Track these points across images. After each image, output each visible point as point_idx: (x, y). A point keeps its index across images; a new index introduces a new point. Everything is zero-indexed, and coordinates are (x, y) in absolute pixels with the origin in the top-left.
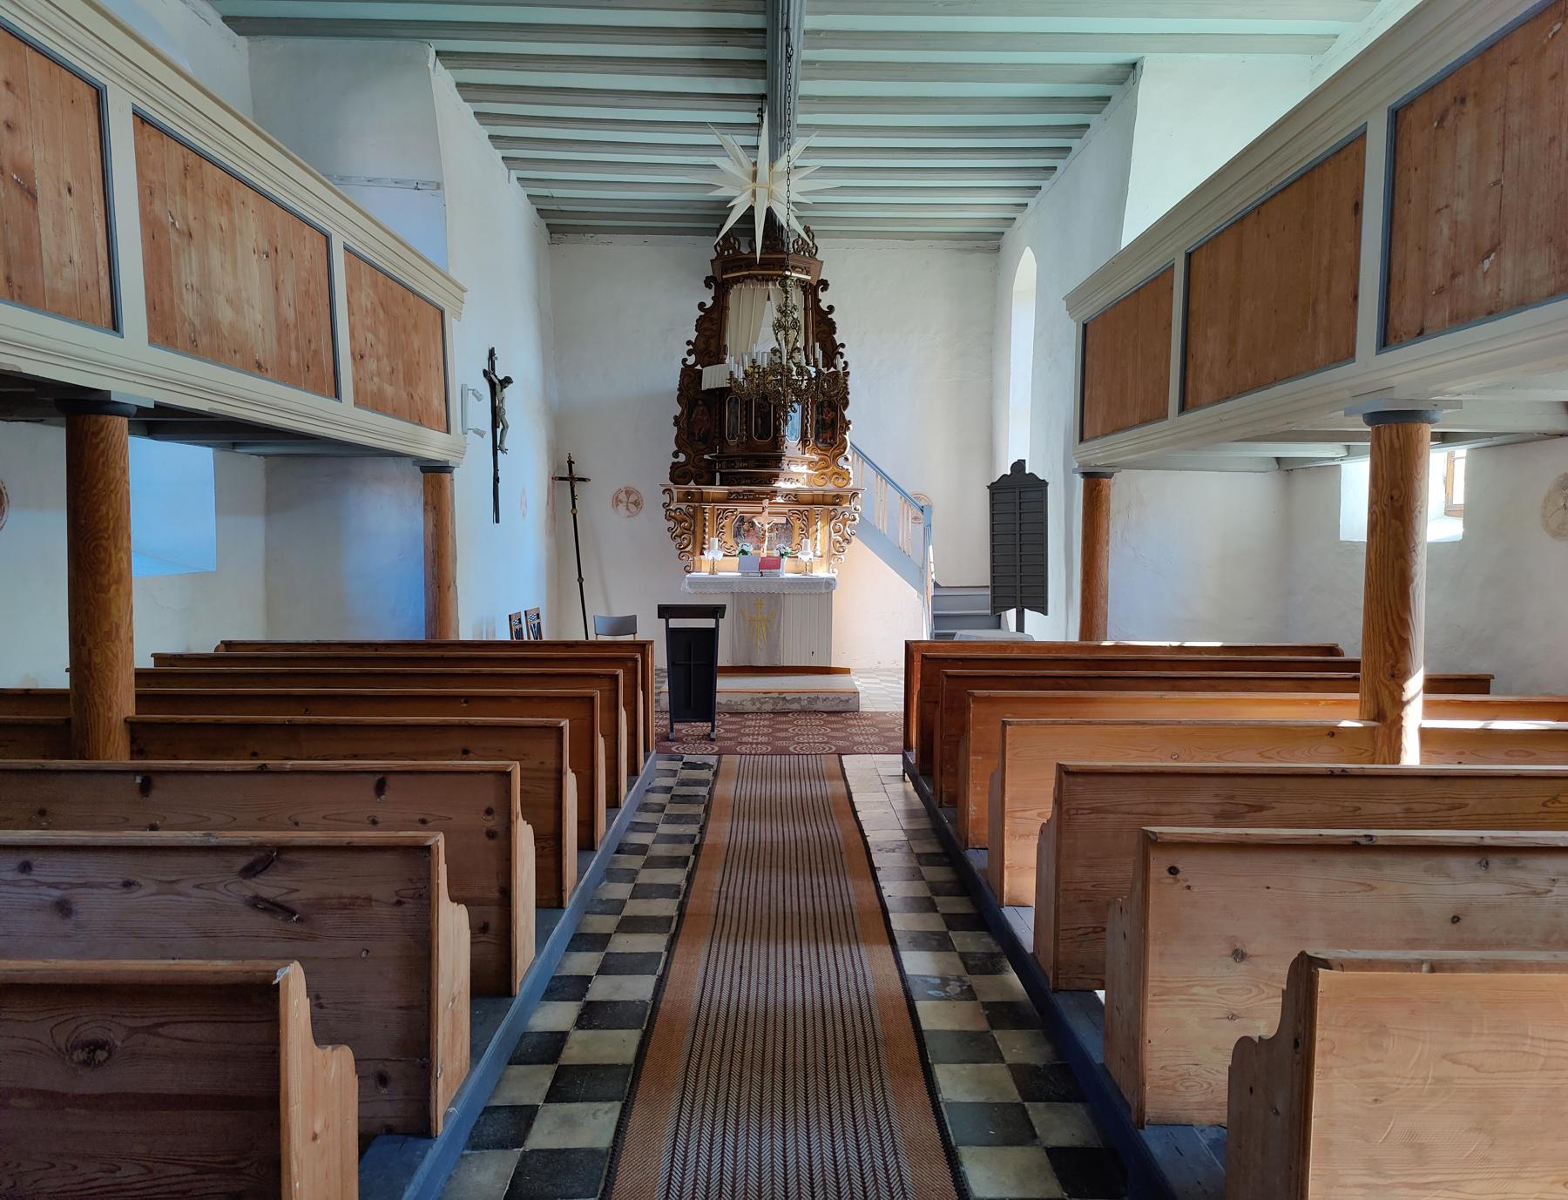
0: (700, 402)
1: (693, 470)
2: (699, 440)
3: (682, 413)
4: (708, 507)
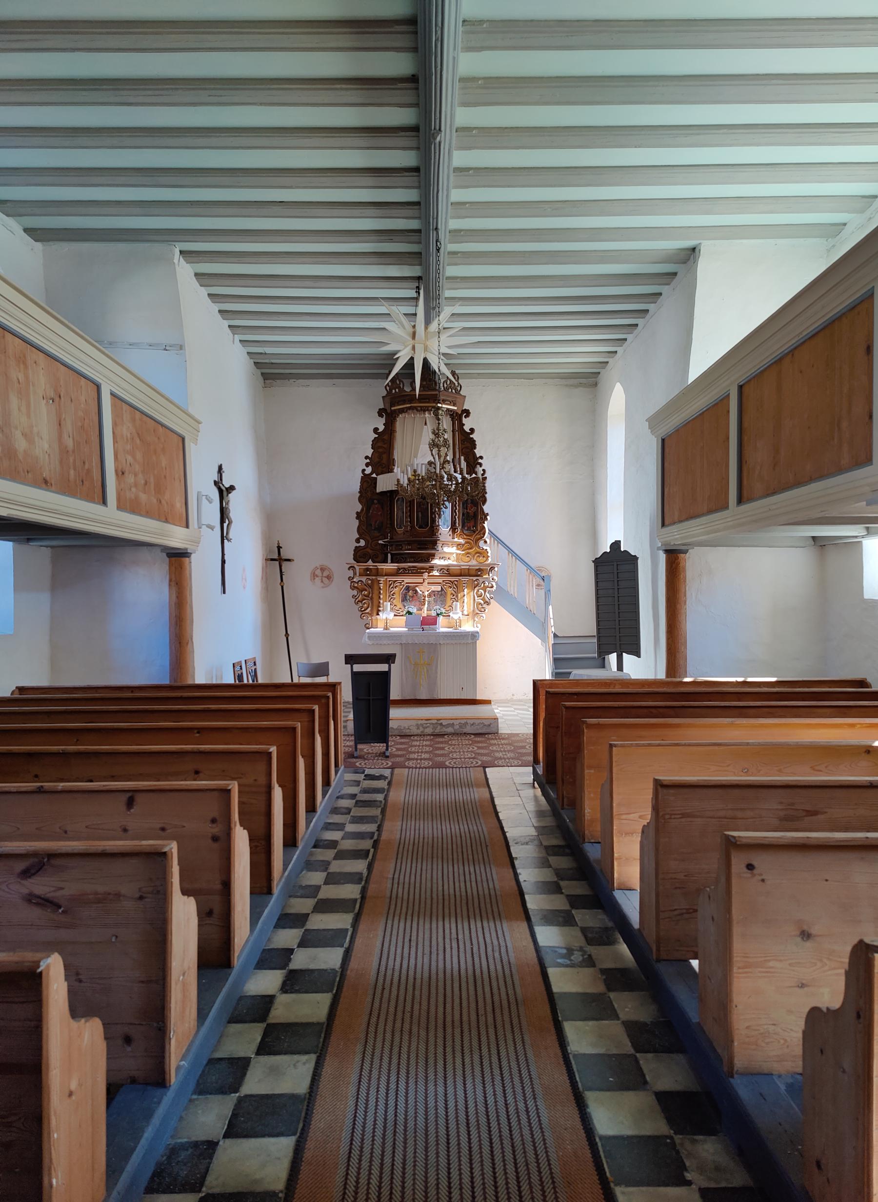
0: (375, 501)
3: (362, 510)
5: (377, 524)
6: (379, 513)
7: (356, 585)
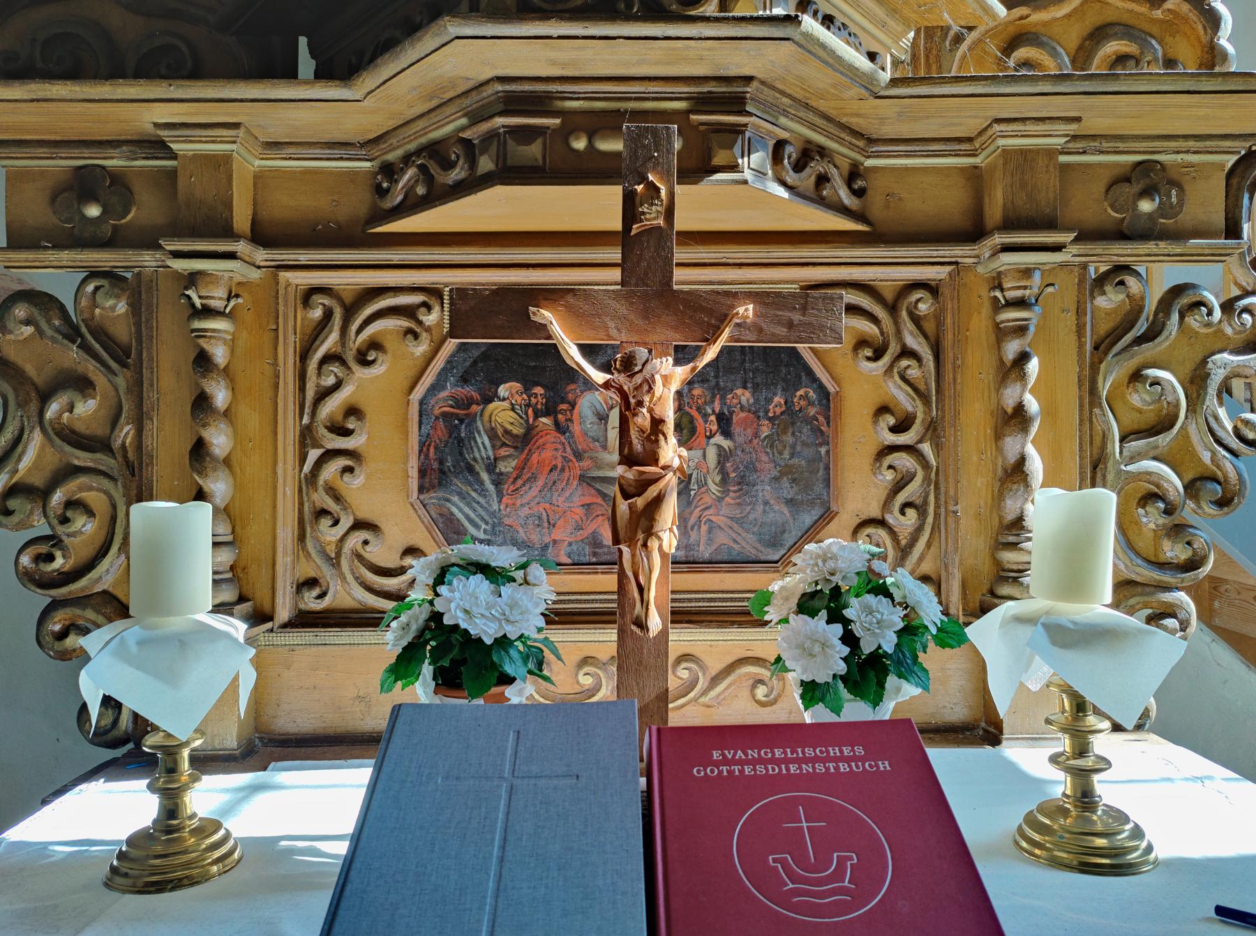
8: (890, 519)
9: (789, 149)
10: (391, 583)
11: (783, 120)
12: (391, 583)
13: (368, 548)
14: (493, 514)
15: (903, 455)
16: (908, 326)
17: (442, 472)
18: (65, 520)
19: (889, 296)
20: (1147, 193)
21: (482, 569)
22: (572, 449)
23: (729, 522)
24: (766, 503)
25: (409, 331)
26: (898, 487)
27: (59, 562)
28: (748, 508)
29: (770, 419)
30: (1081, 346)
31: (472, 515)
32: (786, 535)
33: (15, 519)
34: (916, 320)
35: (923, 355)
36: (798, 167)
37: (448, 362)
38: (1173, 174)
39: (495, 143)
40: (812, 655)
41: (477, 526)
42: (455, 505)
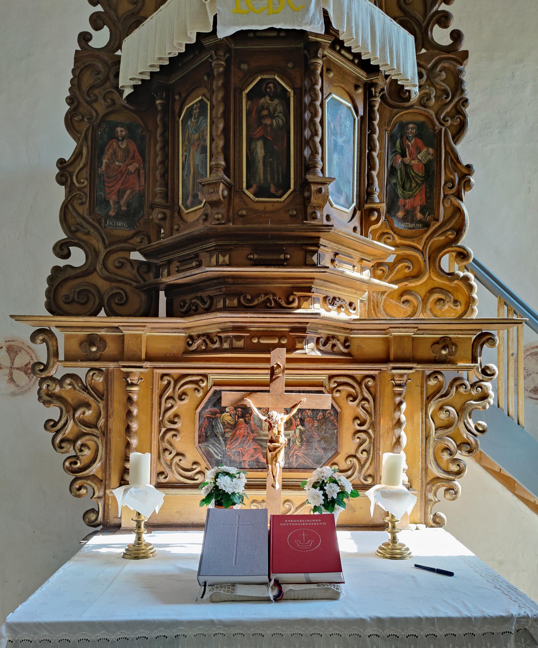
1: (103, 285)
2: (119, 216)
3: (77, 154)
4: (136, 374)
5: (122, 202)
6: (131, 168)
7: (57, 389)
8: (358, 455)
9: (321, 340)
10: (189, 474)
11: (319, 331)
12: (189, 474)
13: (181, 462)
14: (223, 451)
15: (362, 434)
16: (365, 390)
17: (206, 437)
18: (81, 451)
19: (359, 379)
20: (444, 348)
21: (227, 474)
22: (250, 430)
23: (303, 455)
24: (316, 449)
25: (196, 389)
26: (360, 445)
27: (79, 465)
28: (310, 451)
29: (317, 420)
30: (422, 398)
31: (216, 451)
32: (322, 460)
33: (64, 450)
34: (368, 388)
35: (370, 400)
36: (325, 344)
37: (209, 399)
38: (453, 341)
39: (229, 340)
40: (315, 499)
41: (218, 455)
42: (210, 447)
